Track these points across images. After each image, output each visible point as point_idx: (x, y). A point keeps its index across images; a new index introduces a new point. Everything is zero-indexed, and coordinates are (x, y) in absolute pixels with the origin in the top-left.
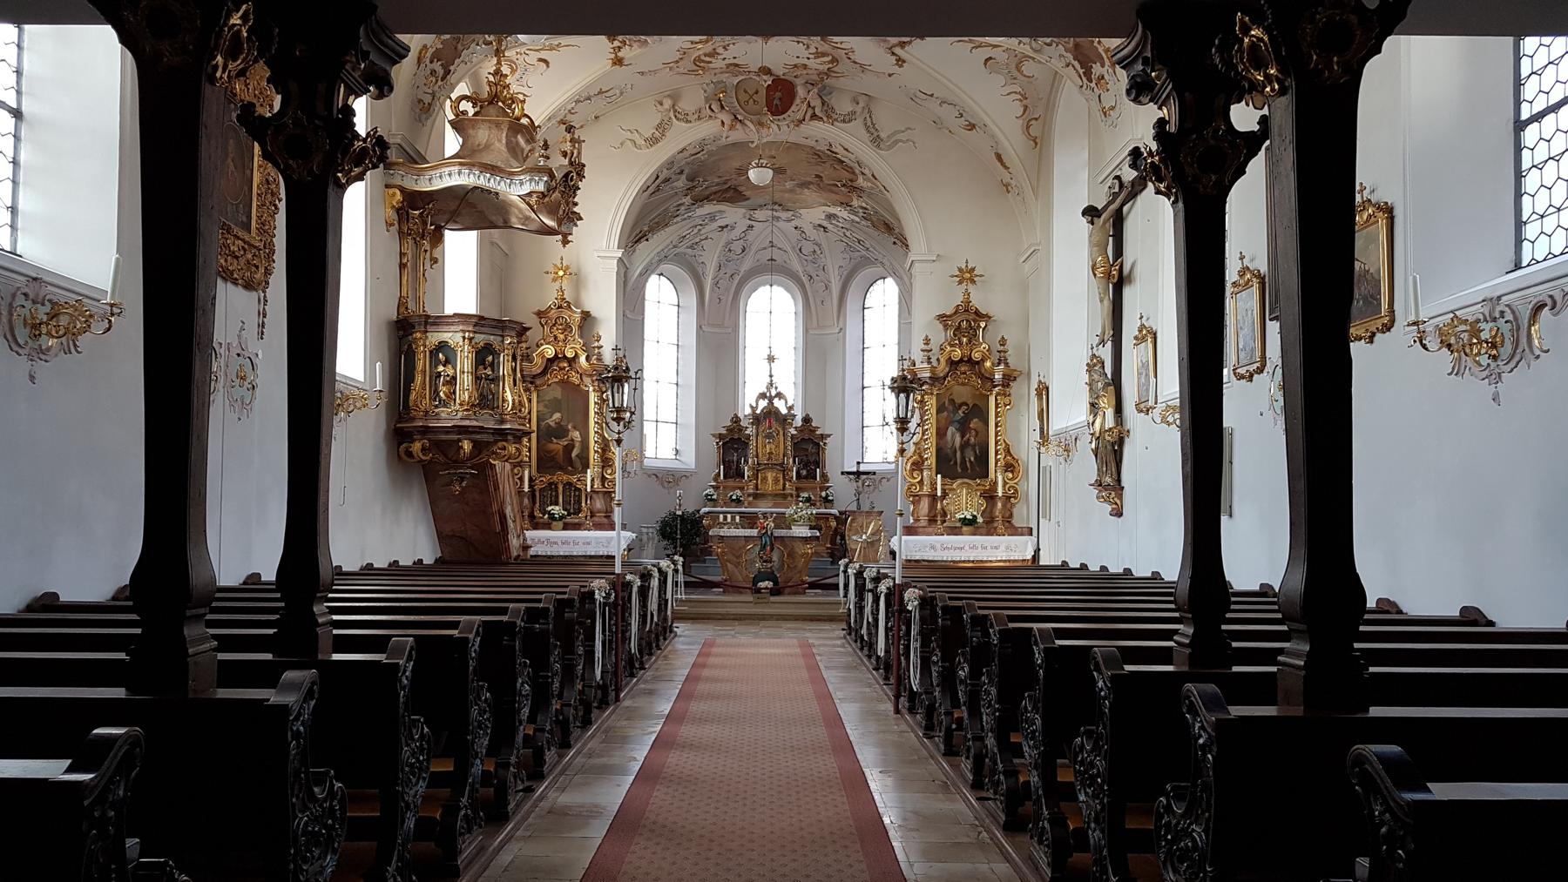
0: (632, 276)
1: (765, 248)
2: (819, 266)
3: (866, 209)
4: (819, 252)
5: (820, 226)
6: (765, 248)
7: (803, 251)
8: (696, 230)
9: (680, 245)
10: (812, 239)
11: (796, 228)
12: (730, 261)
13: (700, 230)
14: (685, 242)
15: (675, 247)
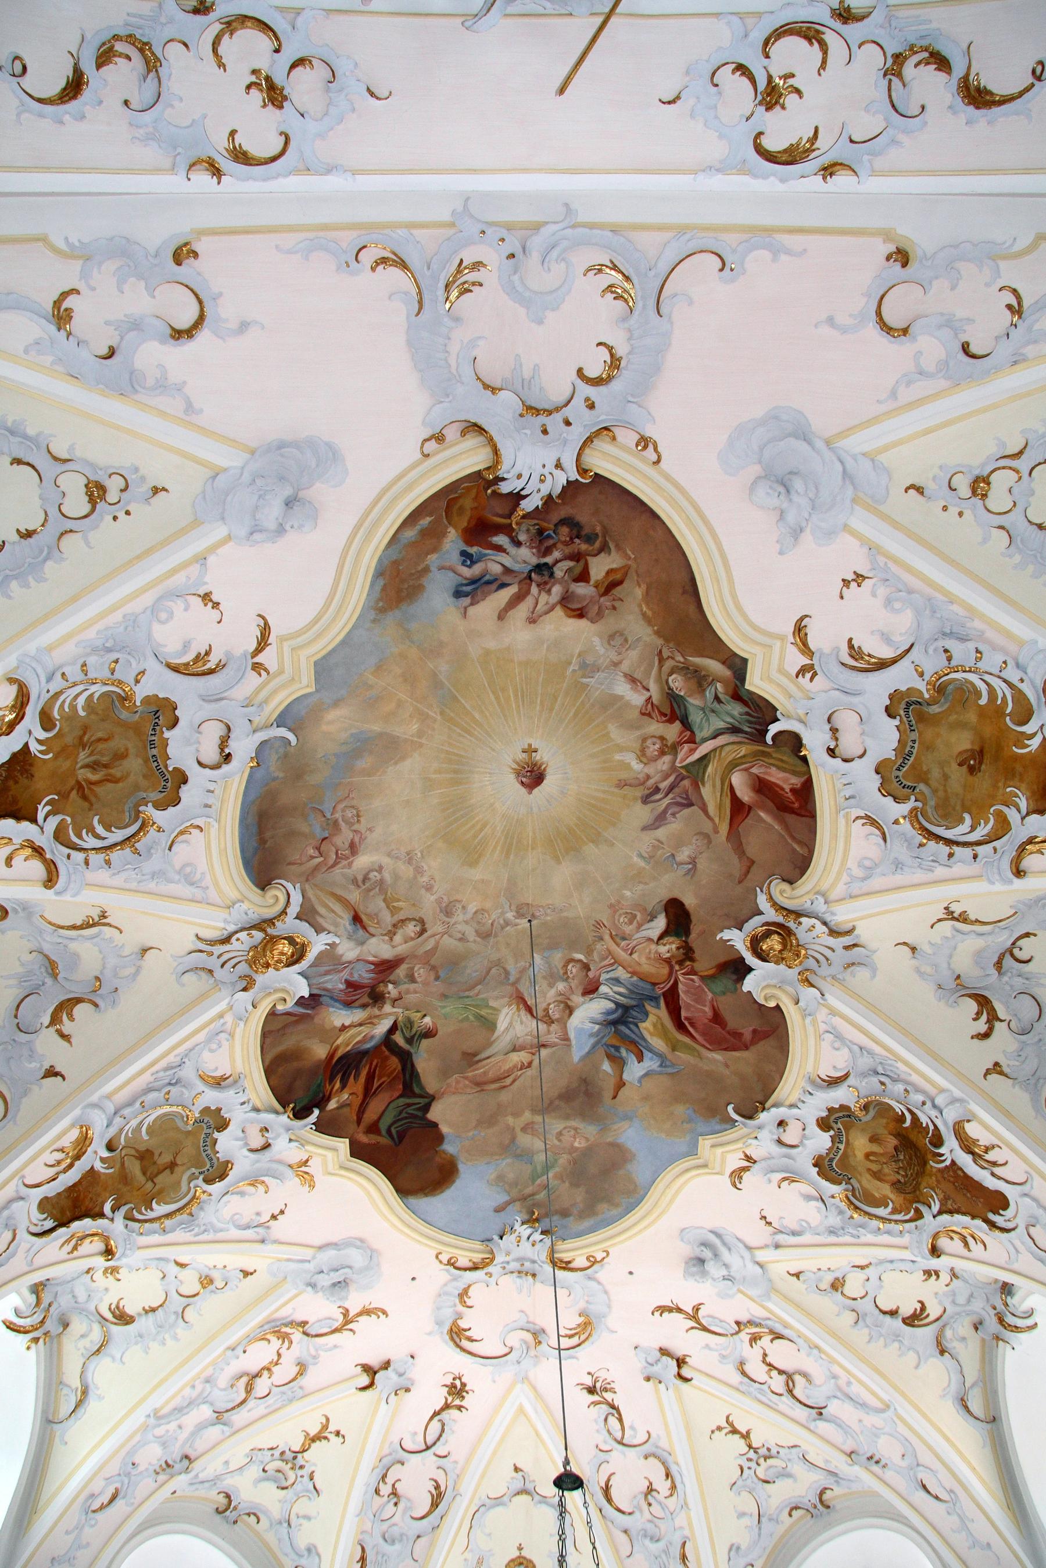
0: (67, 1479)
1: (498, 1501)
2: (666, 1552)
3: (833, 1082)
4: (663, 1486)
5: (664, 1352)
6: (498, 1501)
7: (614, 1493)
8: (285, 1370)
9: (239, 1418)
10: (641, 1437)
11: (591, 1390)
12: (393, 1542)
13: (302, 1368)
14: (254, 1408)
15: (220, 1417)
